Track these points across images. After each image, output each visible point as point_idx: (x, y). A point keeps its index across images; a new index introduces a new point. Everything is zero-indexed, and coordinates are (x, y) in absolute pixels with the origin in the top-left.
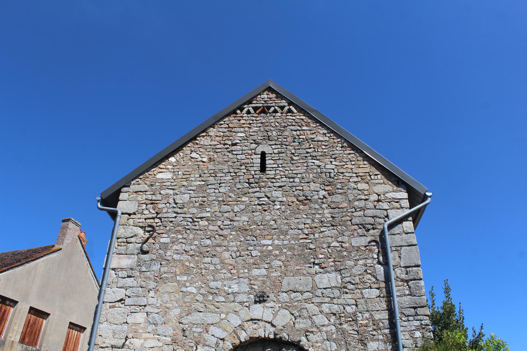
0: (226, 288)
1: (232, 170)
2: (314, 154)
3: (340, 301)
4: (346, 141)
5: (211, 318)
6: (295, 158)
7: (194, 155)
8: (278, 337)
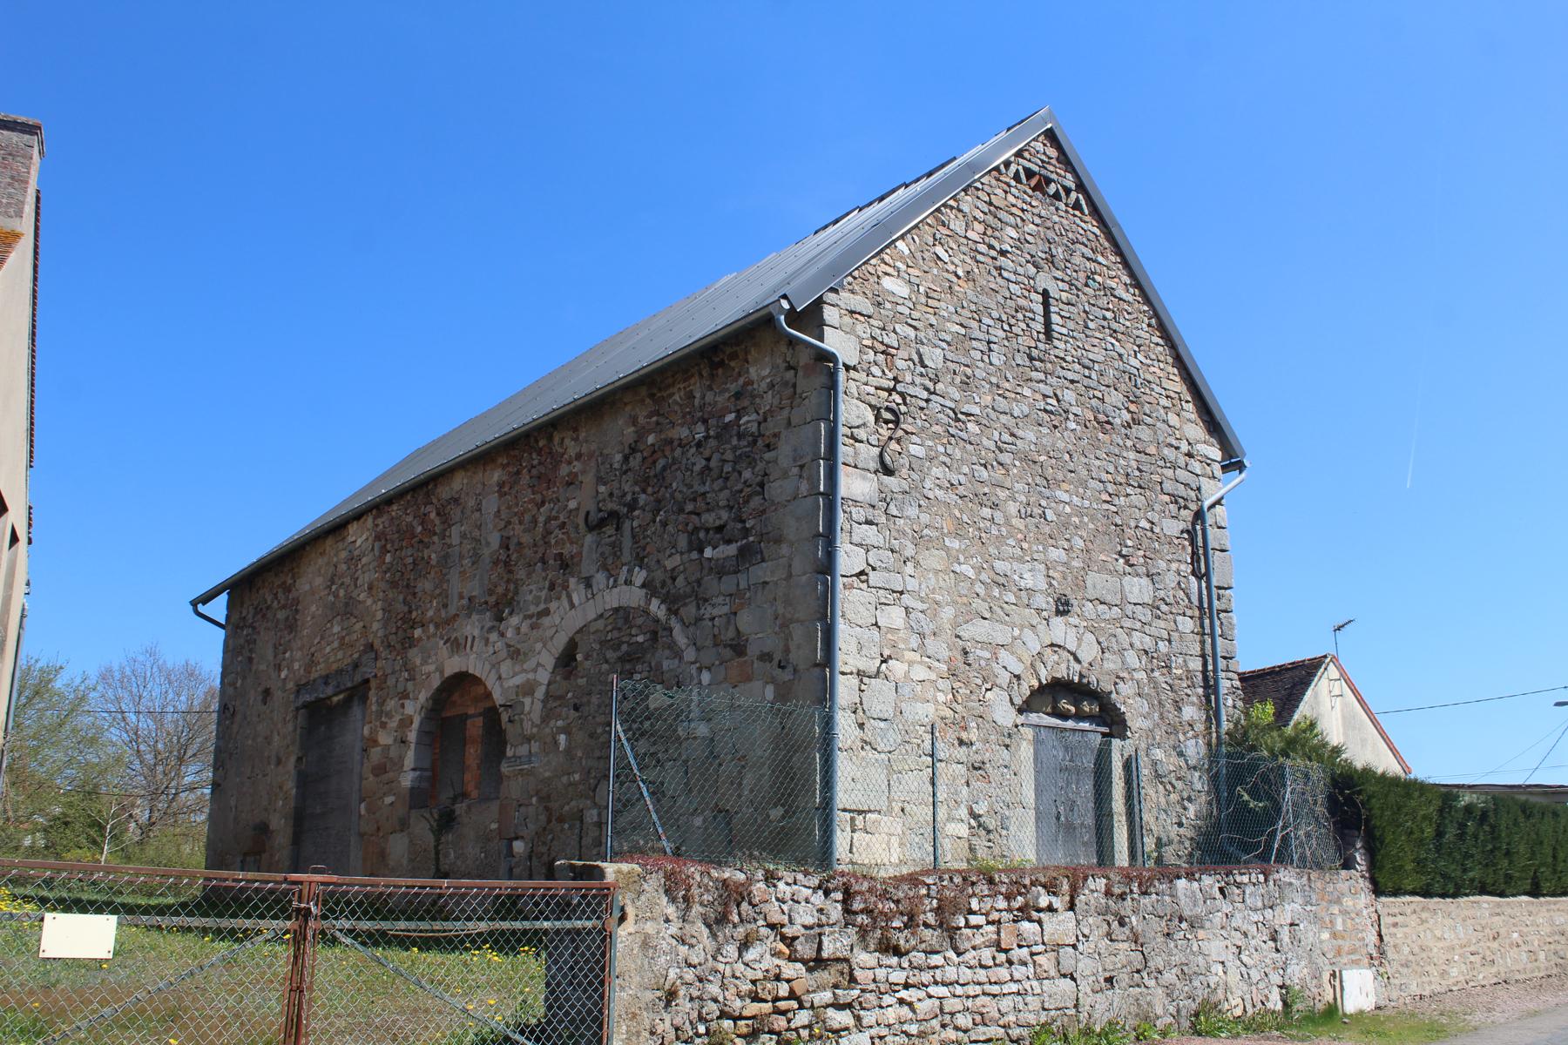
1: (1004, 318)
2: (1115, 326)
3: (1153, 631)
4: (1156, 315)
5: (1001, 634)
6: (1091, 325)
7: (939, 250)
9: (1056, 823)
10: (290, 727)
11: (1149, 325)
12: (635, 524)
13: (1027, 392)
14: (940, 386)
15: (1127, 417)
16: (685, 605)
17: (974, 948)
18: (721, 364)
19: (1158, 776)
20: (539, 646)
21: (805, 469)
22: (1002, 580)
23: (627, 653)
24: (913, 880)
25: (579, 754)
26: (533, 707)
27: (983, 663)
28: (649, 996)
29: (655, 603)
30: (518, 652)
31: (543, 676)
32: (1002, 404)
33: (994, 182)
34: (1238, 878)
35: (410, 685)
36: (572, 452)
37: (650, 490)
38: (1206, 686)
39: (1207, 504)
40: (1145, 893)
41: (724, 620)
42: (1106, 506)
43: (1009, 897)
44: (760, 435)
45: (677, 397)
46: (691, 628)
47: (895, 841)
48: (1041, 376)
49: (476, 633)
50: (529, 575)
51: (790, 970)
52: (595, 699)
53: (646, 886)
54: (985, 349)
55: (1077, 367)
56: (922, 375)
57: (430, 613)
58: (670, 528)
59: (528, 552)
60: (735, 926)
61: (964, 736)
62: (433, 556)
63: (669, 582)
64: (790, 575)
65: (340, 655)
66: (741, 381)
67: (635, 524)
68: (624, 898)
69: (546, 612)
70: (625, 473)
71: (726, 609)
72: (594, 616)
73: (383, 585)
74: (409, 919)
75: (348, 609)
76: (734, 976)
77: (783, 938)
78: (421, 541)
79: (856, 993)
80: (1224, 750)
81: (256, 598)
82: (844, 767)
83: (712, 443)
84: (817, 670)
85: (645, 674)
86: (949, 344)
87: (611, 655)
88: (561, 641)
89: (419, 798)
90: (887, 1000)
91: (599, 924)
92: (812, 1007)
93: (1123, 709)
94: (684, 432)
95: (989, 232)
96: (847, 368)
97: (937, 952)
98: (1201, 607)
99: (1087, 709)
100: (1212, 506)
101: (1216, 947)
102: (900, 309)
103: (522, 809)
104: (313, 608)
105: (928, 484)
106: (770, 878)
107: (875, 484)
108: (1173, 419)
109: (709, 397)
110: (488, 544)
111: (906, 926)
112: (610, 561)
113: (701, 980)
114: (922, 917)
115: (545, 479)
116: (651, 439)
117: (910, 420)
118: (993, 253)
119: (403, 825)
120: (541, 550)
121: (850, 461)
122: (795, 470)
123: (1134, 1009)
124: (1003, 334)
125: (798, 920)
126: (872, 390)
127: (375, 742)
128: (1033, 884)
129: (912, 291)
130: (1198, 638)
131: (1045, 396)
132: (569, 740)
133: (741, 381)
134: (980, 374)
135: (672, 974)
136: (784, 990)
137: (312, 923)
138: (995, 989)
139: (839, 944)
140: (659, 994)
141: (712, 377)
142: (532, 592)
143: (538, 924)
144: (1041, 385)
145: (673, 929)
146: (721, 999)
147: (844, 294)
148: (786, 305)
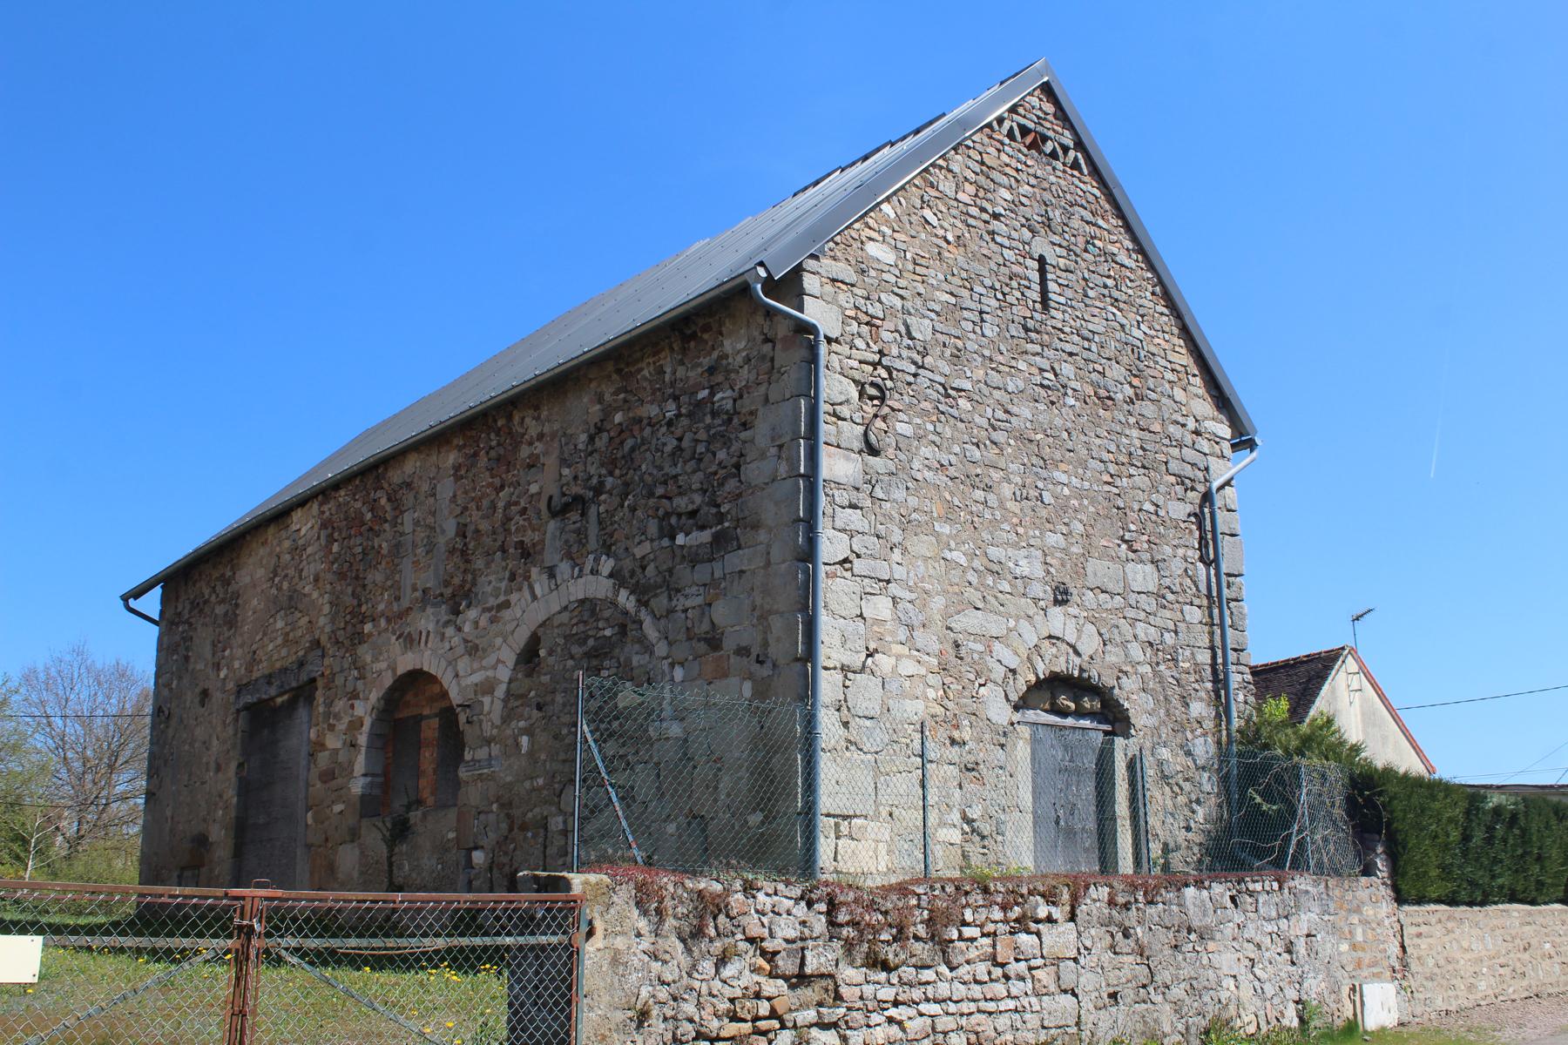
0: (1011, 565)
1: (998, 286)
2: (1116, 294)
3: (1158, 621)
4: (1161, 282)
5: (995, 626)
6: (1091, 293)
7: (928, 213)
8: (1085, 675)
9: (1054, 827)
10: (230, 731)
11: (1153, 294)
12: (602, 509)
13: (1022, 365)
14: (928, 360)
15: (1130, 392)
16: (656, 595)
17: (968, 962)
18: (694, 336)
19: (1164, 777)
20: (499, 641)
21: (783, 449)
22: (996, 568)
23: (594, 648)
24: (902, 890)
25: (543, 757)
26: (492, 706)
27: (976, 656)
28: (620, 1016)
29: (623, 594)
30: (476, 648)
31: (504, 674)
32: (995, 378)
33: (986, 140)
34: (1251, 886)
35: (360, 684)
36: (533, 432)
37: (617, 472)
38: (1215, 681)
39: (1215, 485)
40: (1151, 903)
41: (697, 612)
42: (1107, 488)
43: (1005, 908)
44: (736, 413)
45: (646, 372)
46: (663, 621)
47: (882, 848)
48: (1038, 348)
49: (431, 627)
50: (488, 565)
51: (771, 987)
52: (559, 698)
53: (615, 898)
54: (977, 319)
55: (1076, 338)
56: (909, 348)
57: (381, 607)
58: (639, 513)
59: (487, 540)
60: (711, 941)
61: (956, 734)
62: (384, 545)
63: (639, 571)
64: (768, 564)
65: (284, 652)
66: (715, 355)
67: (602, 509)
68: (592, 912)
69: (506, 605)
70: (591, 454)
71: (699, 600)
72: (558, 608)
73: (329, 577)
74: (360, 936)
75: (292, 603)
76: (710, 994)
77: (764, 953)
78: (371, 529)
79: (842, 1011)
80: (1235, 749)
81: (192, 589)
82: (827, 769)
83: (684, 421)
84: (798, 665)
85: (613, 670)
86: (938, 314)
87: (577, 650)
88: (522, 637)
89: (370, 806)
90: (876, 1018)
91: (565, 939)
92: (795, 1027)
93: (1126, 705)
94: (653, 410)
95: (981, 194)
96: (829, 340)
97: (929, 967)
98: (1209, 596)
99: (1088, 706)
100: (1222, 487)
101: (1226, 960)
102: (886, 276)
103: (482, 817)
104: (255, 602)
105: (916, 465)
106: (749, 889)
107: (860, 465)
108: (1179, 394)
109: (681, 372)
110: (443, 531)
111: (895, 939)
112: (574, 549)
113: (675, 999)
114: (912, 929)
115: (503, 462)
116: (618, 418)
117: (897, 396)
118: (985, 216)
119: (354, 835)
120: (500, 538)
121: (833, 440)
122: (773, 451)
123: (1139, 1027)
124: (997, 304)
125: (779, 933)
126: (855, 364)
127: (321, 745)
128: (1030, 893)
129: (898, 257)
130: (1206, 629)
131: (1042, 370)
132: (532, 743)
133: (715, 355)
134: (971, 346)
135: (644, 992)
136: (764, 1008)
137: (255, 942)
138: (991, 1006)
139: (823, 959)
140: (630, 1014)
141: (684, 350)
142: (491, 583)
143: (499, 940)
144: (1038, 358)
145: (645, 944)
146: (697, 1018)
147: (825, 261)
148: (762, 272)
